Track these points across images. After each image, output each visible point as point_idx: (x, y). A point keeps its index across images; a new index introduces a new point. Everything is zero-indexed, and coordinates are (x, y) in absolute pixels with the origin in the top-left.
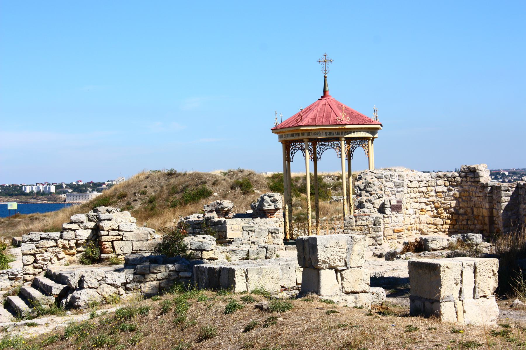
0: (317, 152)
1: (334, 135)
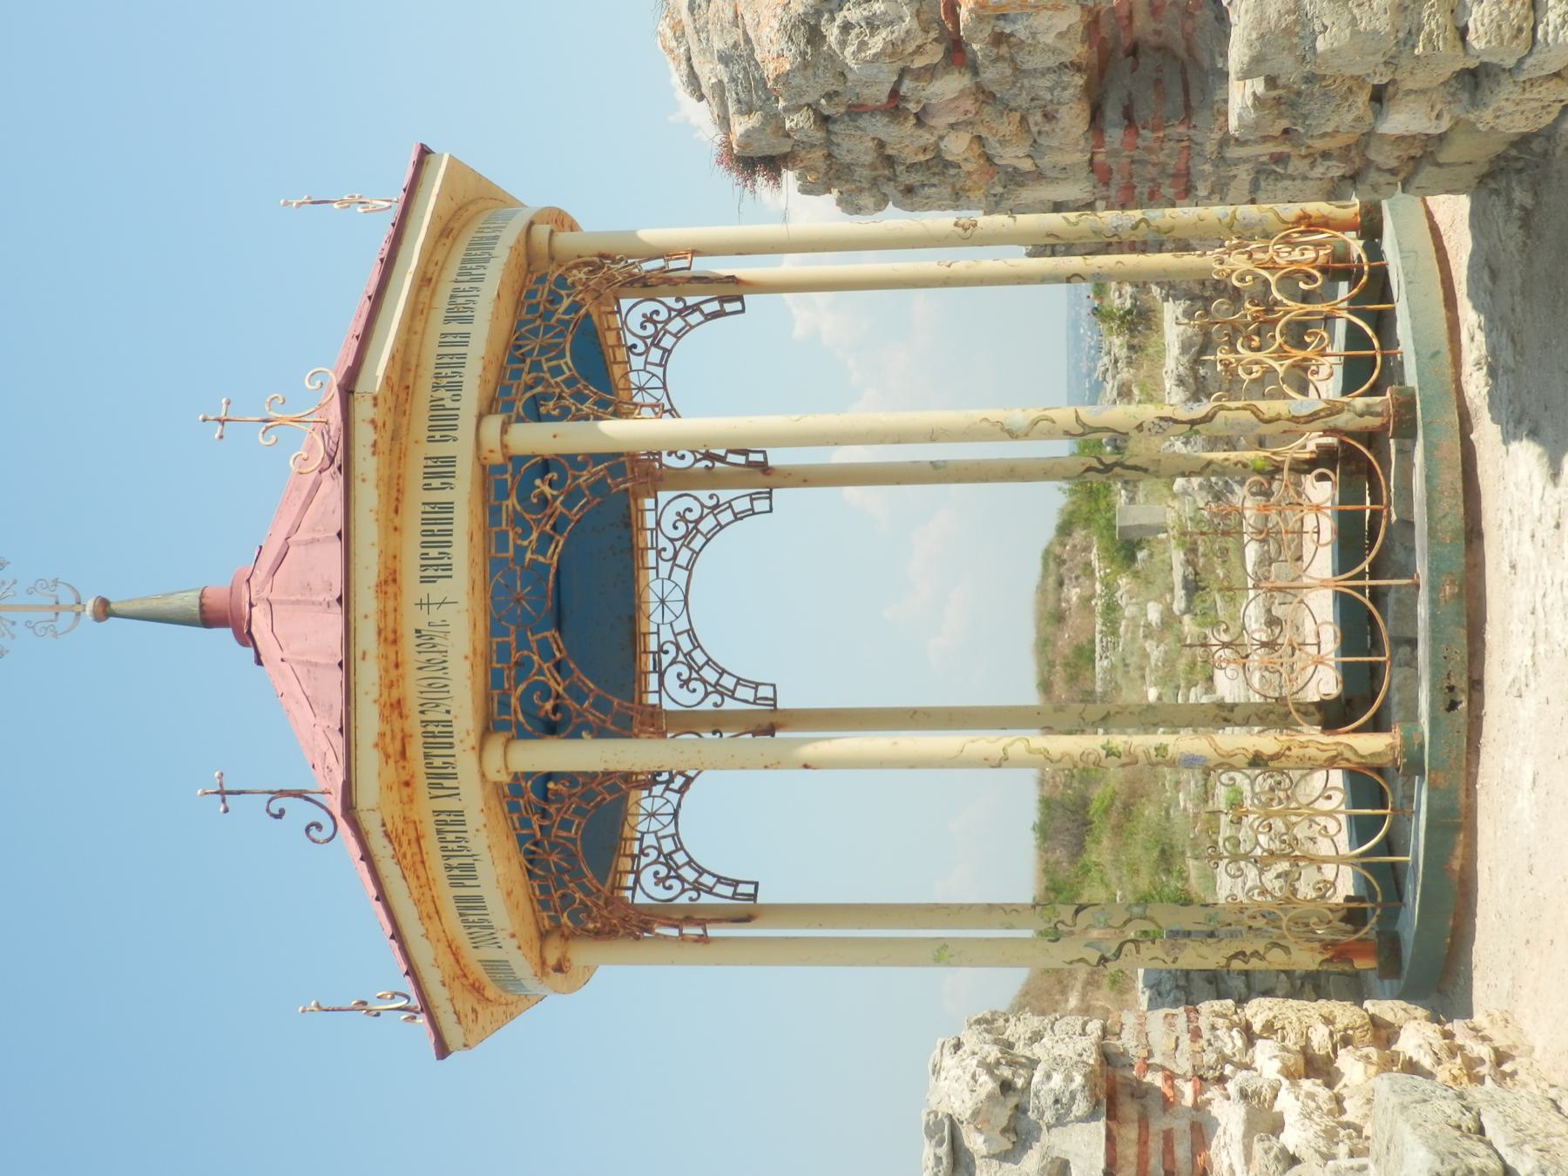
0: (707, 705)
1: (448, 507)
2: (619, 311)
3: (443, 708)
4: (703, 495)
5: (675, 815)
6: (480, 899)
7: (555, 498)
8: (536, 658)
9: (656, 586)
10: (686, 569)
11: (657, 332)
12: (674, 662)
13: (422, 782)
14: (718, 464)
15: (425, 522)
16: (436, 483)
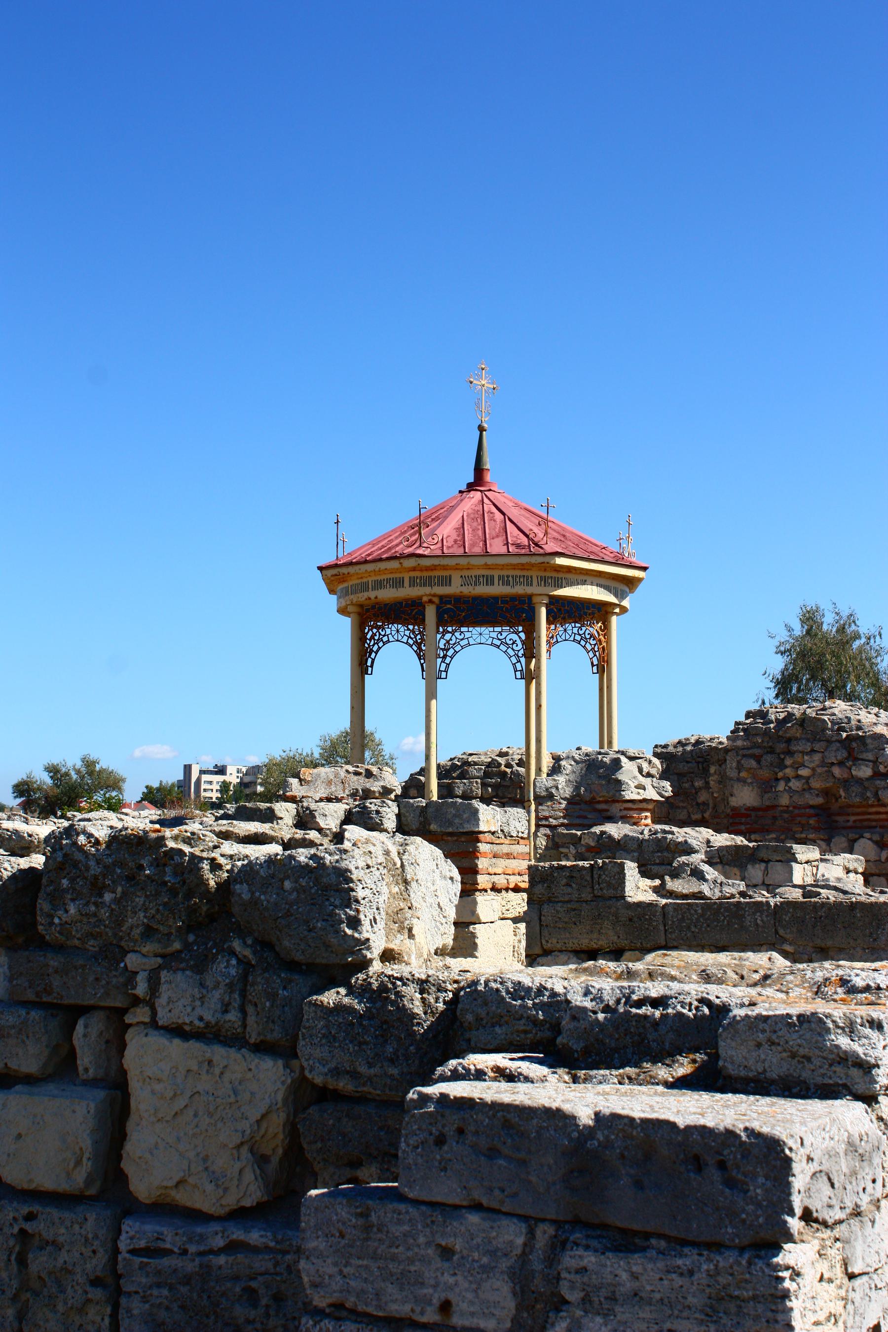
6: (493, 584)
13: (543, 574)
14: (439, 660)
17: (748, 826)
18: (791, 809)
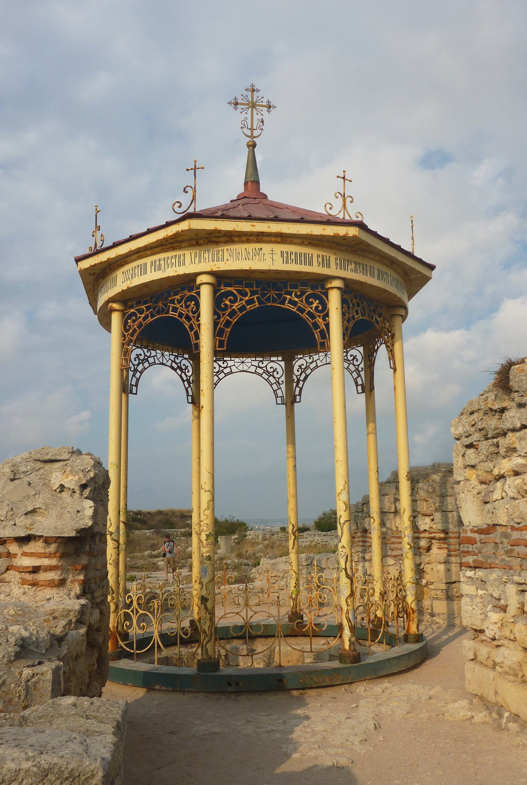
1: (311, 264)
2: (357, 347)
3: (229, 258)
4: (283, 379)
5: (162, 364)
6: (145, 273)
7: (312, 308)
8: (247, 298)
9: (249, 360)
10: (255, 371)
11: (349, 361)
12: (220, 366)
14: (295, 384)
15: (305, 254)
16: (320, 260)
17: (475, 557)
18: (509, 530)
